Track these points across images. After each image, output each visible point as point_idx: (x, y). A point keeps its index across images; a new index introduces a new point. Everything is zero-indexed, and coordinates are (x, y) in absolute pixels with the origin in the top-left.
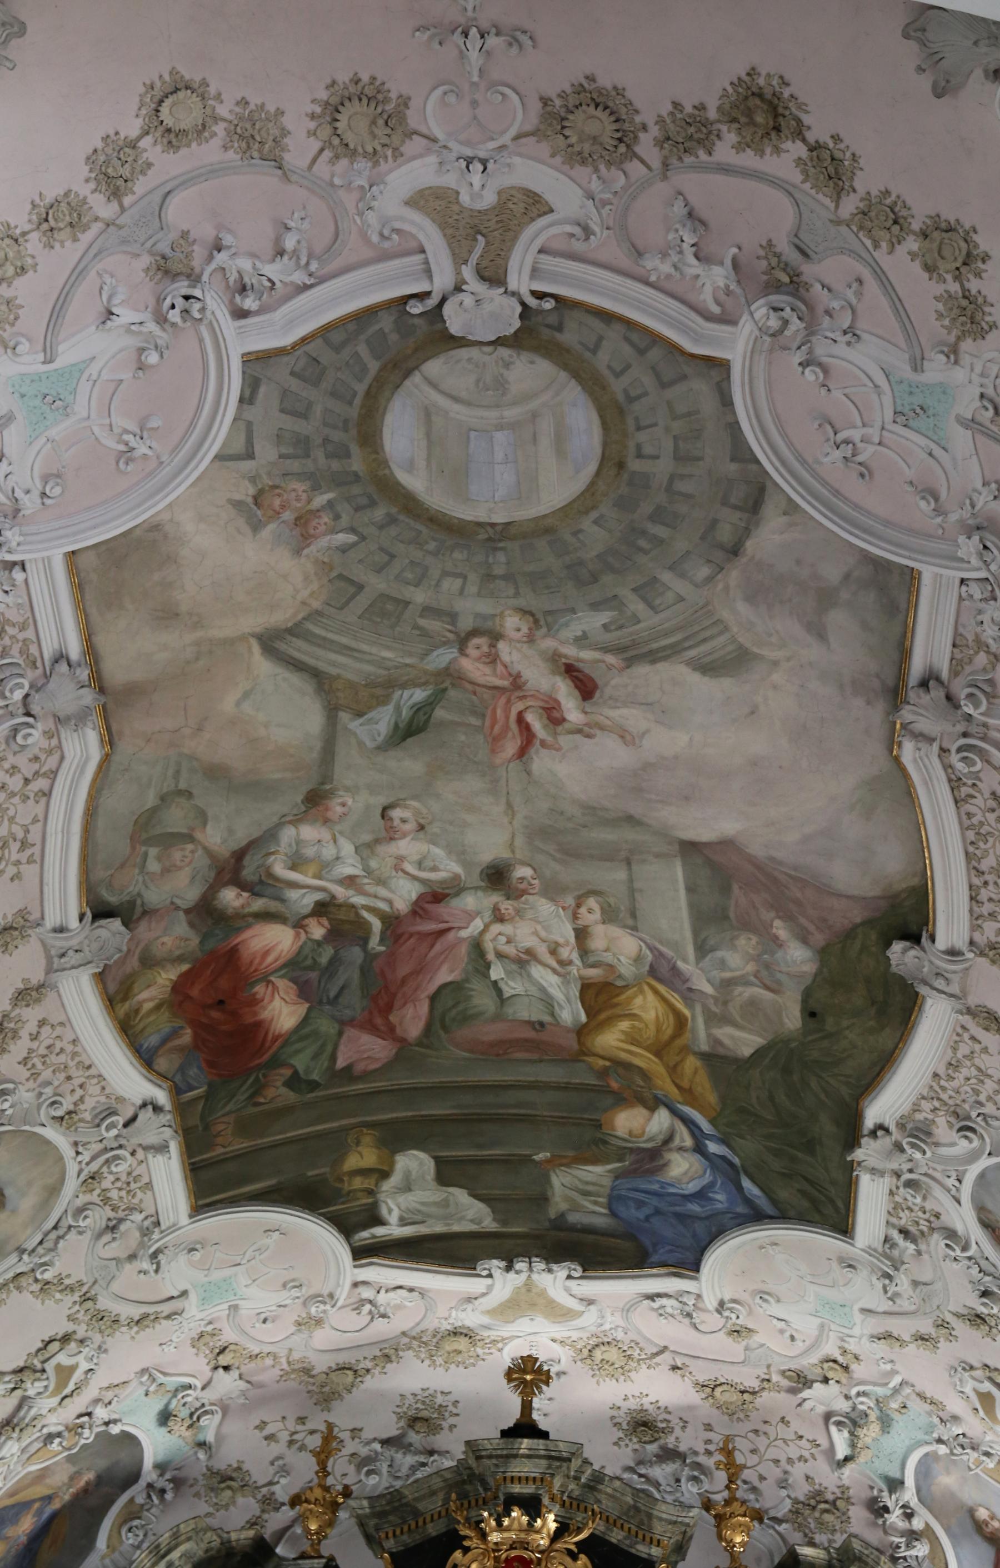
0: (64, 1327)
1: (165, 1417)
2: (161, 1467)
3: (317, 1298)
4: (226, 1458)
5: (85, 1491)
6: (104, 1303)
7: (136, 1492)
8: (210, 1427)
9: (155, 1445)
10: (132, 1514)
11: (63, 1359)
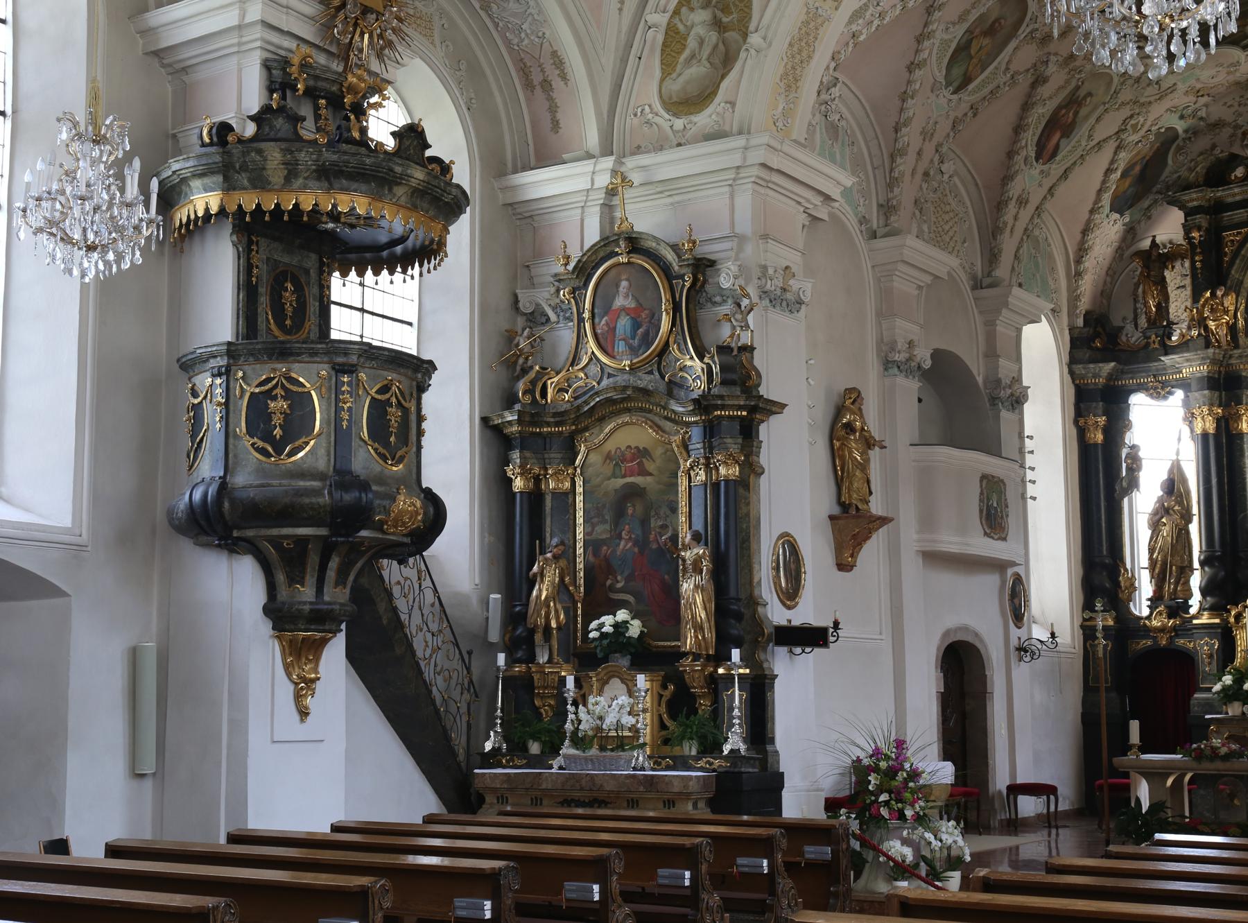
0: (1129, 114)
1: (1182, 117)
2: (1186, 131)
3: (1232, 65)
4: (1212, 119)
5: (1158, 149)
6: (1142, 100)
7: (1179, 141)
8: (1203, 113)
9: (1180, 126)
10: (1179, 149)
11: (1133, 122)
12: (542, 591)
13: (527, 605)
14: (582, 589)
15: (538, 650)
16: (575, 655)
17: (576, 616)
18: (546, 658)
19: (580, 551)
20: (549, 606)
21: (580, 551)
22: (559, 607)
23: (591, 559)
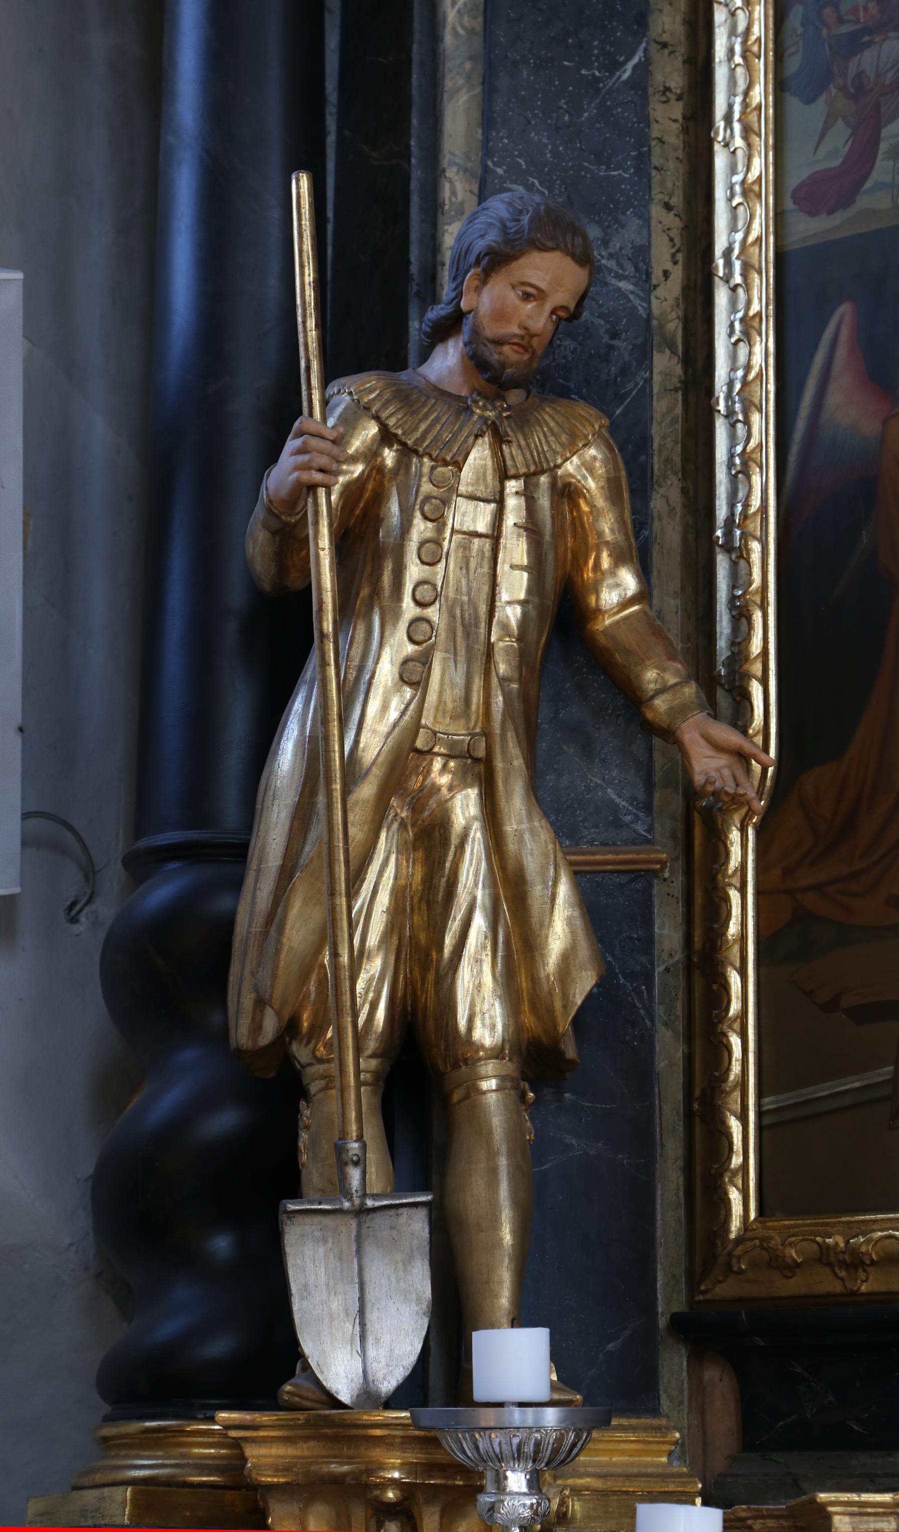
12: (384, 693)
13: (232, 854)
14: (762, 698)
15: (313, 1267)
16: (705, 1332)
17: (705, 962)
18: (397, 1342)
19: (743, 356)
20: (431, 840)
21: (743, 356)
22: (530, 836)
23: (848, 408)
